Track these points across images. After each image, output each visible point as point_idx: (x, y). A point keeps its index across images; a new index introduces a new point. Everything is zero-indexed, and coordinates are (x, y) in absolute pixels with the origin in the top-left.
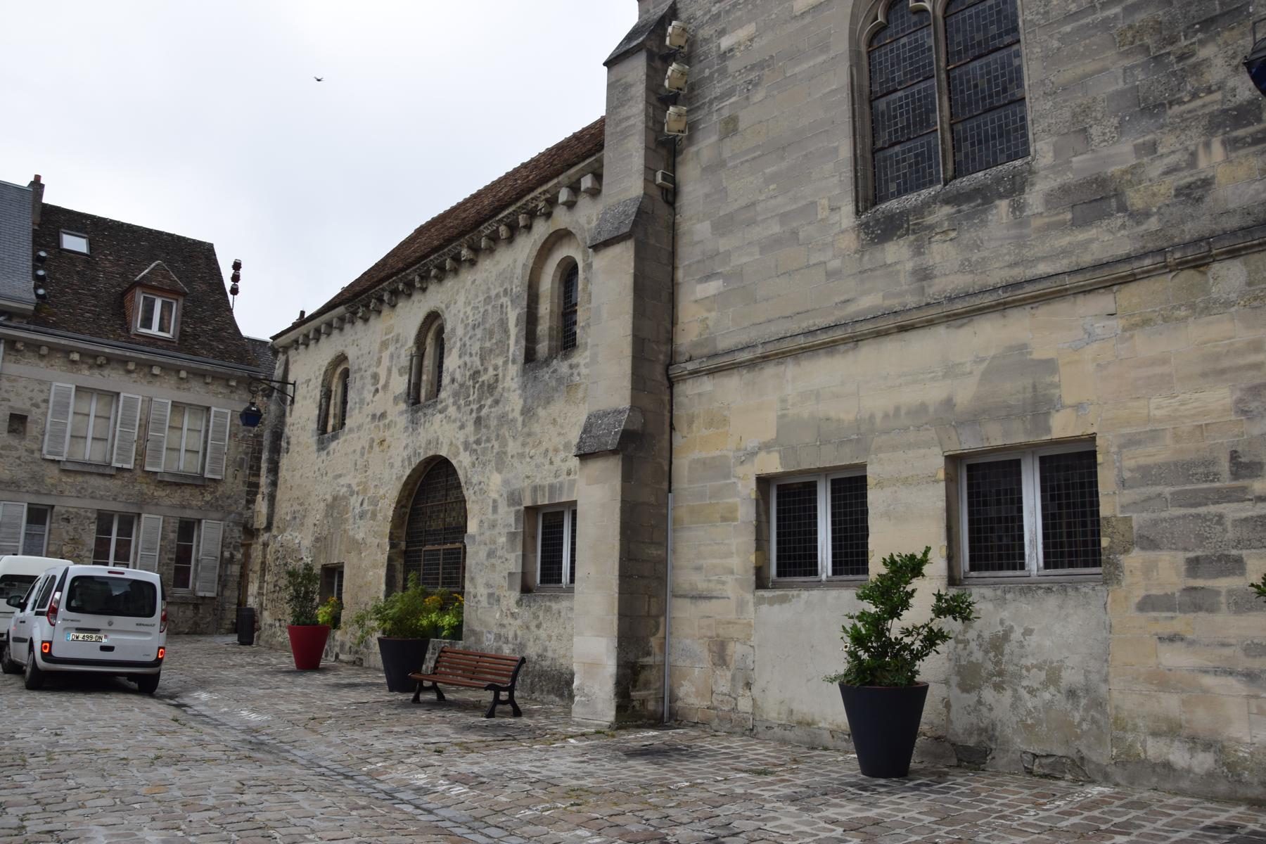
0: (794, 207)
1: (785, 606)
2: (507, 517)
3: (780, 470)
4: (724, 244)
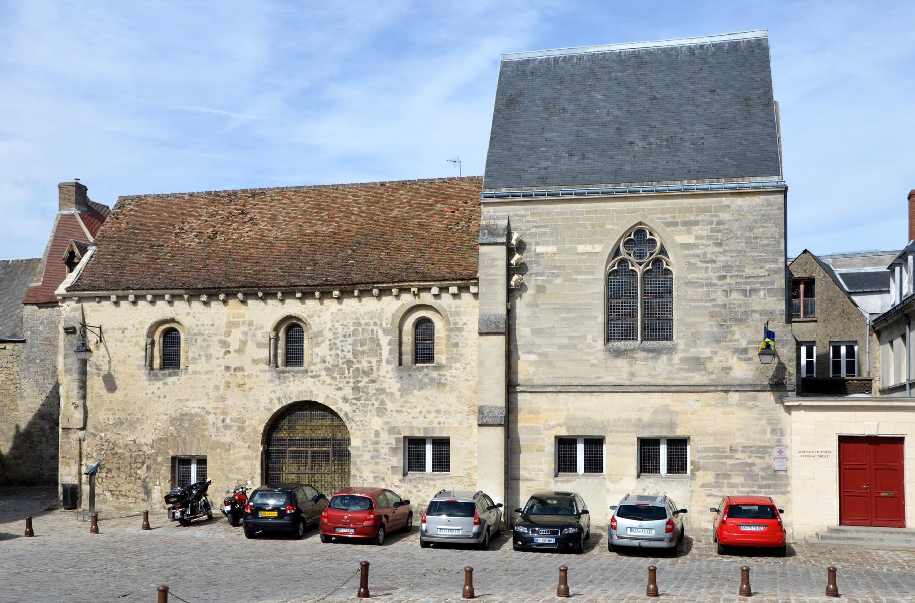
0: (575, 335)
1: (569, 484)
2: (388, 441)
3: (566, 434)
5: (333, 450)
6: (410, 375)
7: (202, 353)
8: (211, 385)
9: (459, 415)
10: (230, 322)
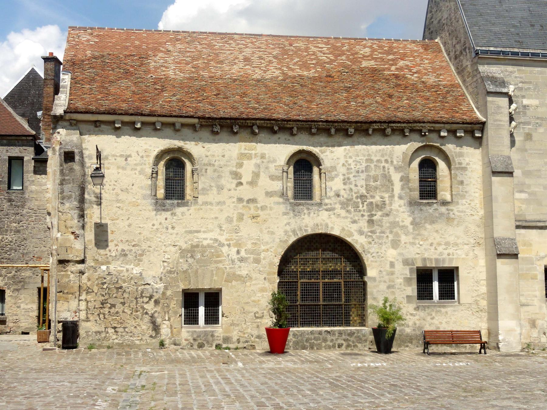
4: (527, 181)
5: (344, 282)
6: (421, 210)
7: (213, 184)
8: (223, 217)
9: (466, 246)
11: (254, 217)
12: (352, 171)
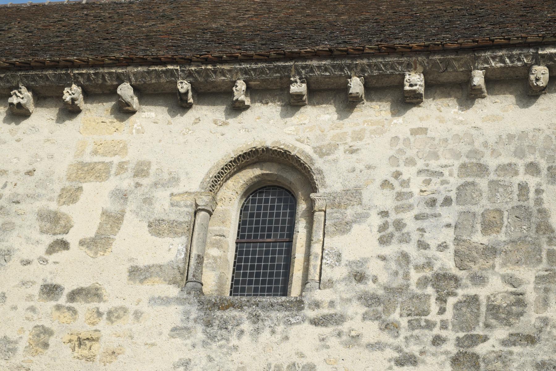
10: (83, 165)
11: (81, 342)
12: (411, 201)
